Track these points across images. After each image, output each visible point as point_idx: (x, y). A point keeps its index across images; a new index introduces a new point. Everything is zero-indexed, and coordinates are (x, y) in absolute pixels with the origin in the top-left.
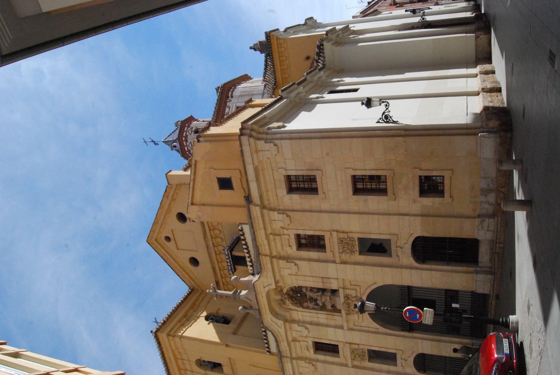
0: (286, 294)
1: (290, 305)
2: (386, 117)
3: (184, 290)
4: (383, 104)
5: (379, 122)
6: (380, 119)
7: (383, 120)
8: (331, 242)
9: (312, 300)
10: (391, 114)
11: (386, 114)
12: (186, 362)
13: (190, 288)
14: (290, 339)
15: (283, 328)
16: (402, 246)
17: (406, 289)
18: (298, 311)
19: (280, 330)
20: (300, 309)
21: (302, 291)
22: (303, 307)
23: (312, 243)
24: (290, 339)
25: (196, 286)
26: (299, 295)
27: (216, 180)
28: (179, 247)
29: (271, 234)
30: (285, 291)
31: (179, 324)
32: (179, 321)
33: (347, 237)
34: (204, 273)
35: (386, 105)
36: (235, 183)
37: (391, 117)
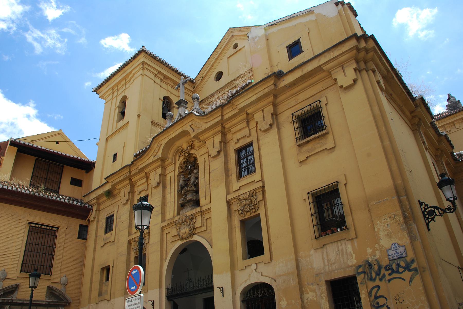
0: (189, 154)
1: (180, 161)
2: (432, 213)
3: (192, 75)
4: (449, 204)
5: (421, 204)
6: (426, 205)
7: (425, 209)
8: (249, 182)
9: (187, 181)
10: (437, 218)
11: (436, 211)
12: (124, 87)
13: (195, 79)
14: (147, 170)
15: (156, 158)
16: (257, 270)
17: (210, 285)
18: (174, 171)
19: (152, 157)
20: (177, 173)
21: (195, 169)
22: (179, 176)
23: (245, 160)
24: (147, 170)
25: (197, 85)
26: (189, 167)
27: (296, 39)
28: (229, 59)
29: (248, 114)
30: (192, 151)
31: (156, 73)
32: (159, 72)
33: (258, 200)
34: (211, 86)
35: (449, 209)
36: (298, 60)
37: (433, 219)
